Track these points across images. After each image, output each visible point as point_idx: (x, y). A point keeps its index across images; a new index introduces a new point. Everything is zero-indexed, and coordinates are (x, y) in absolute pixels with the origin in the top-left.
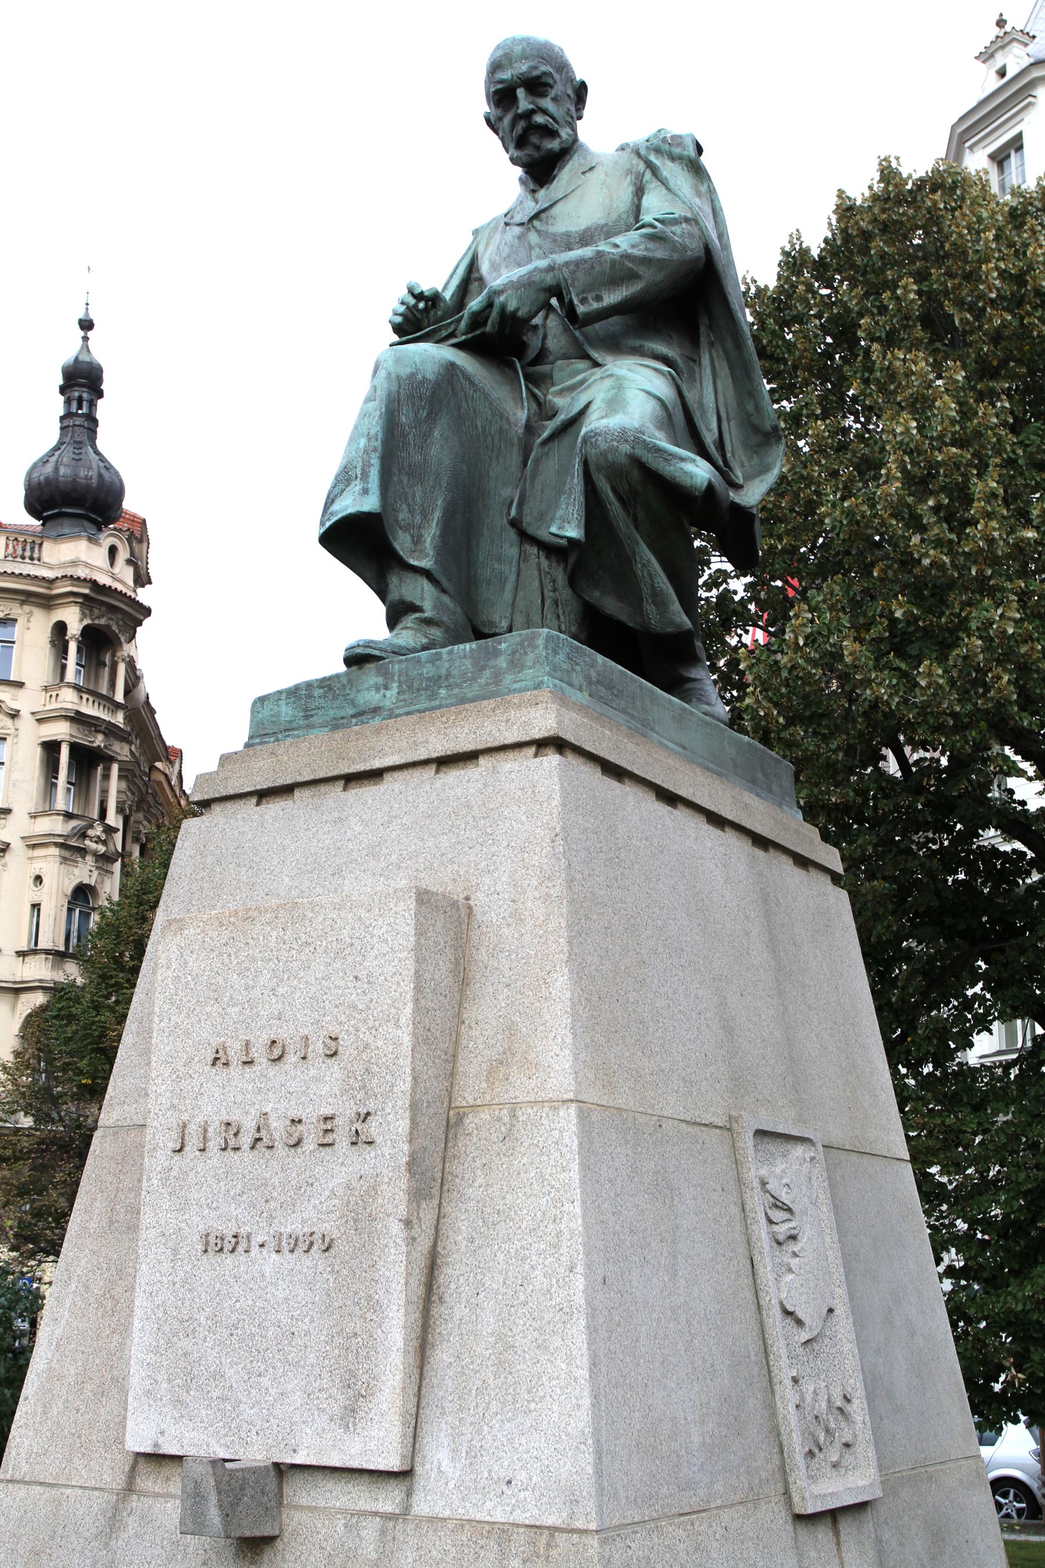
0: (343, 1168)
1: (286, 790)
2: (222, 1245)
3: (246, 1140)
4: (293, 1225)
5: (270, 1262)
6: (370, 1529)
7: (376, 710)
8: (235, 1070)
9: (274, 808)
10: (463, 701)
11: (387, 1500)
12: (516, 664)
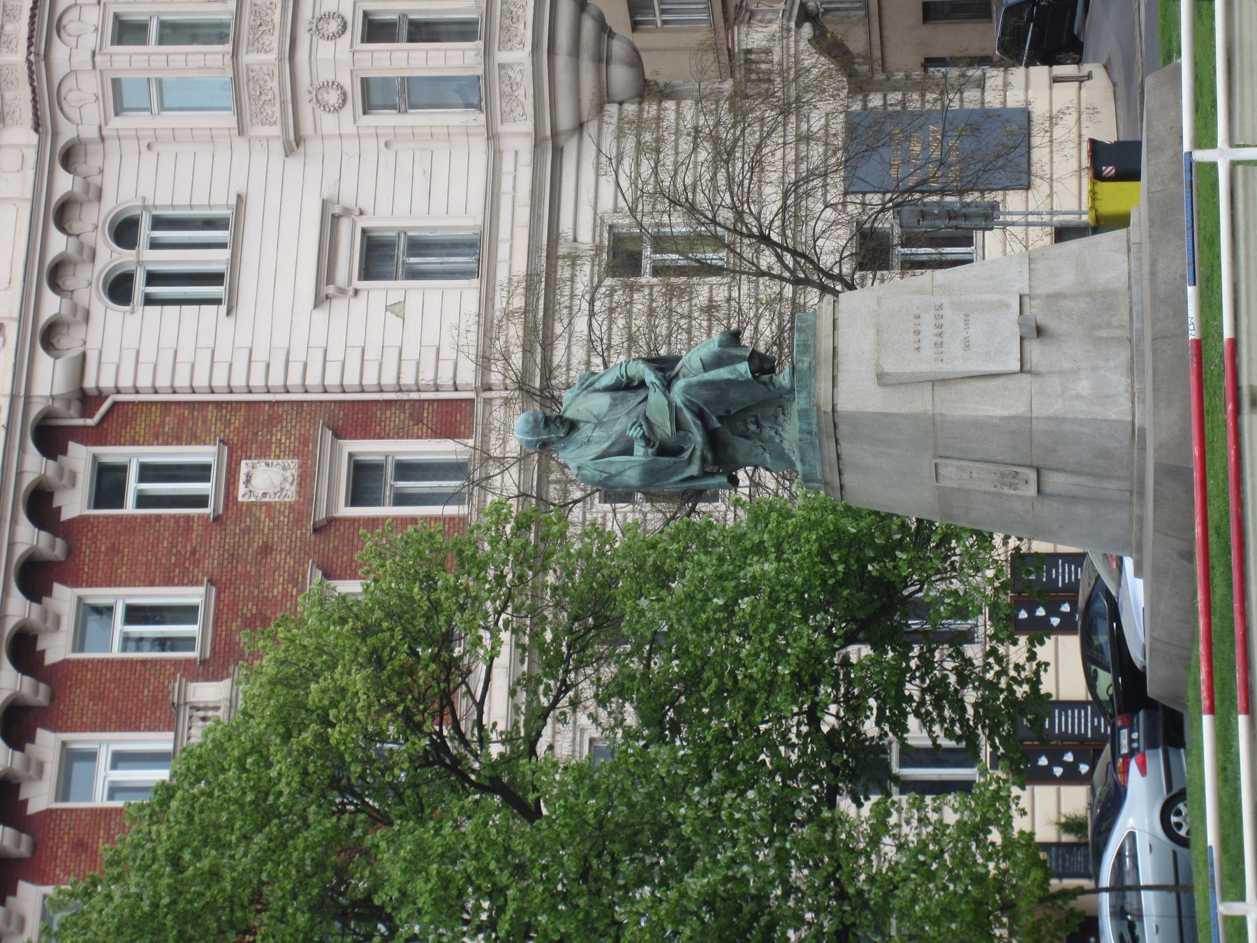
0: (947, 311)
1: (834, 378)
2: (967, 346)
3: (939, 340)
4: (963, 326)
5: (971, 331)
6: (1033, 302)
7: (810, 363)
8: (921, 345)
9: (840, 377)
10: (815, 335)
11: (1026, 300)
12: (805, 321)
